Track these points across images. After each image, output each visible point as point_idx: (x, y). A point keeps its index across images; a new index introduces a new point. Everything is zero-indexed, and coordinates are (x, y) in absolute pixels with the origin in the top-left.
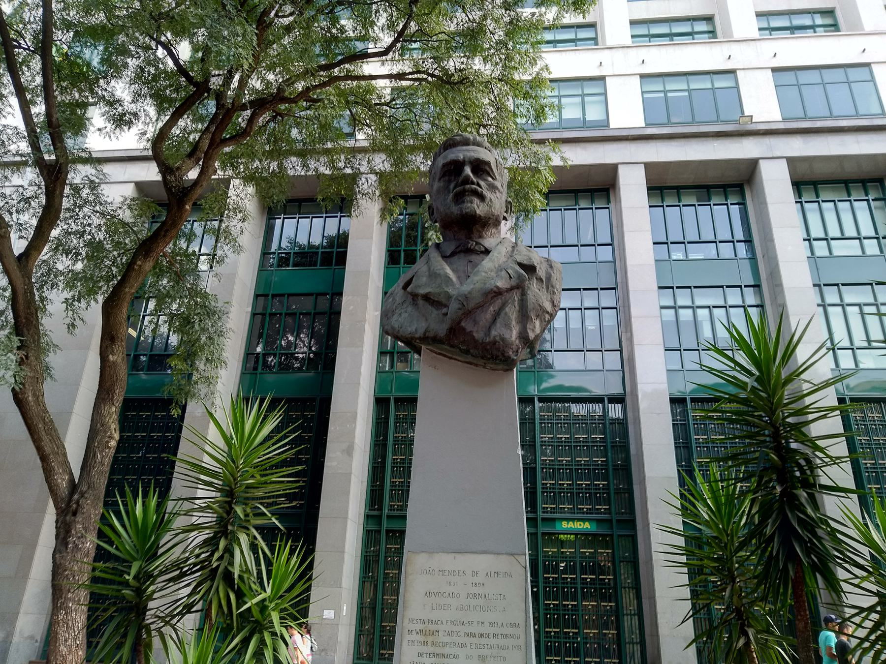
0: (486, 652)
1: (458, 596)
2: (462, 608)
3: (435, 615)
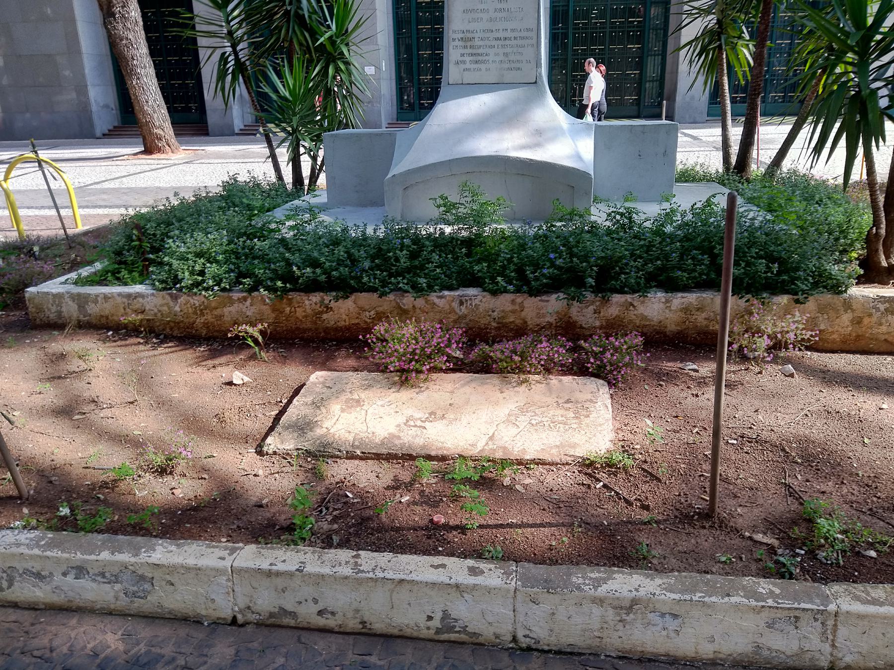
0: (508, 50)
1: (488, 11)
2: (491, 20)
3: (472, 26)
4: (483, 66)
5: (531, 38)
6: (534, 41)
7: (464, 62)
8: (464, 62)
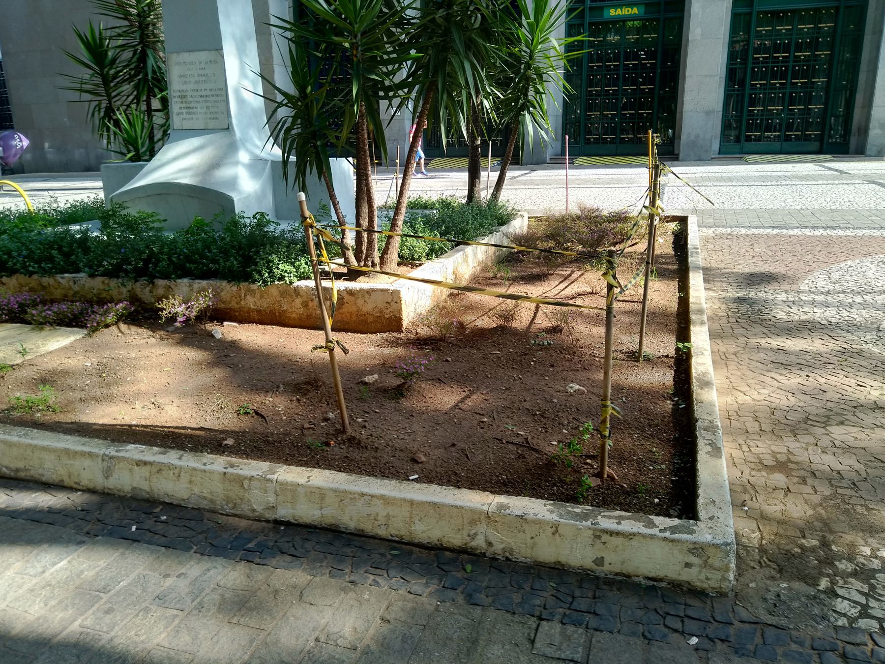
0: (209, 104)
2: (196, 82)
3: (184, 87)
4: (194, 116)
5: (220, 95)
6: (224, 98)
7: (182, 113)
8: (182, 113)
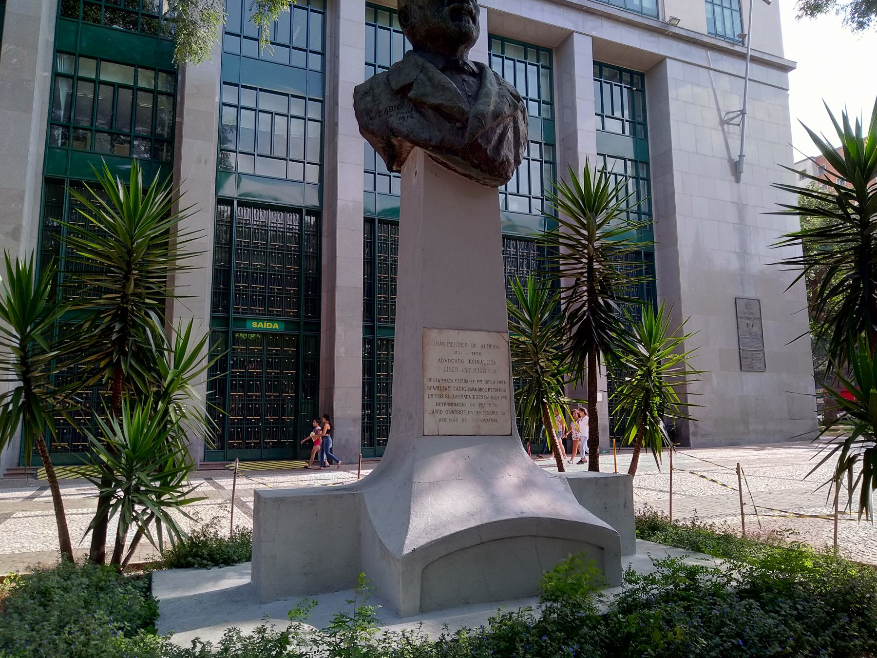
3: (446, 376)
4: (458, 416)
7: (440, 412)
8: (440, 412)
